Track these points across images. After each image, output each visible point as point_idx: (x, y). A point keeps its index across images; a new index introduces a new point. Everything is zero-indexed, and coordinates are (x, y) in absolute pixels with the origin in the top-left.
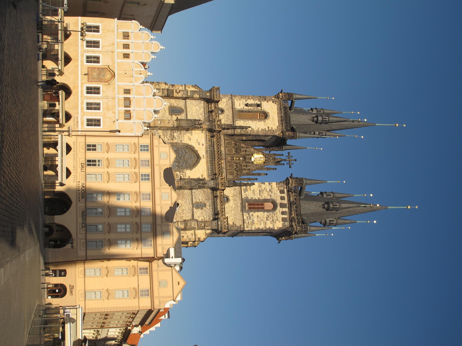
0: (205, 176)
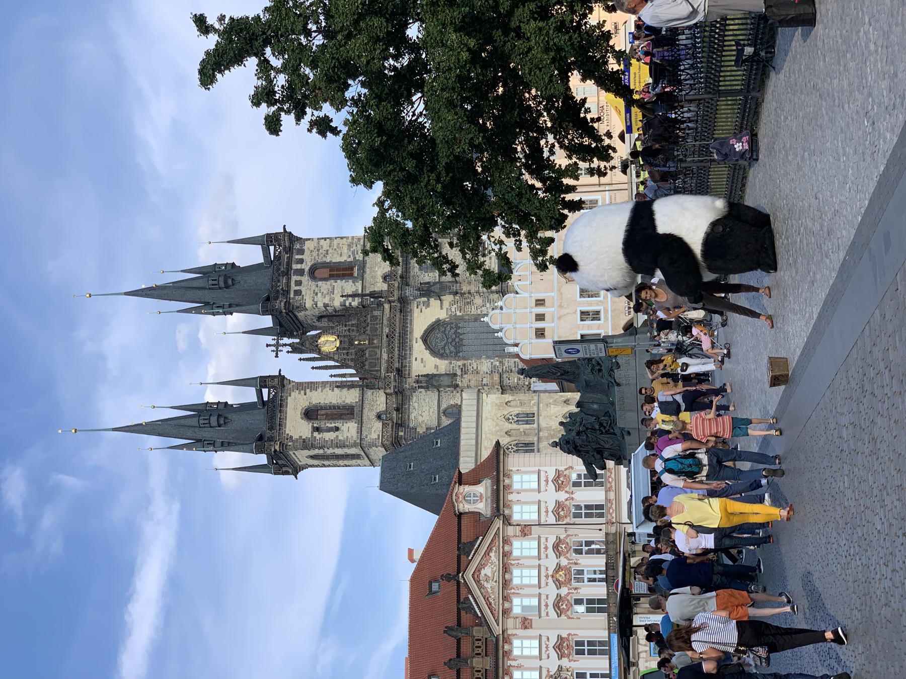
0: (416, 312)
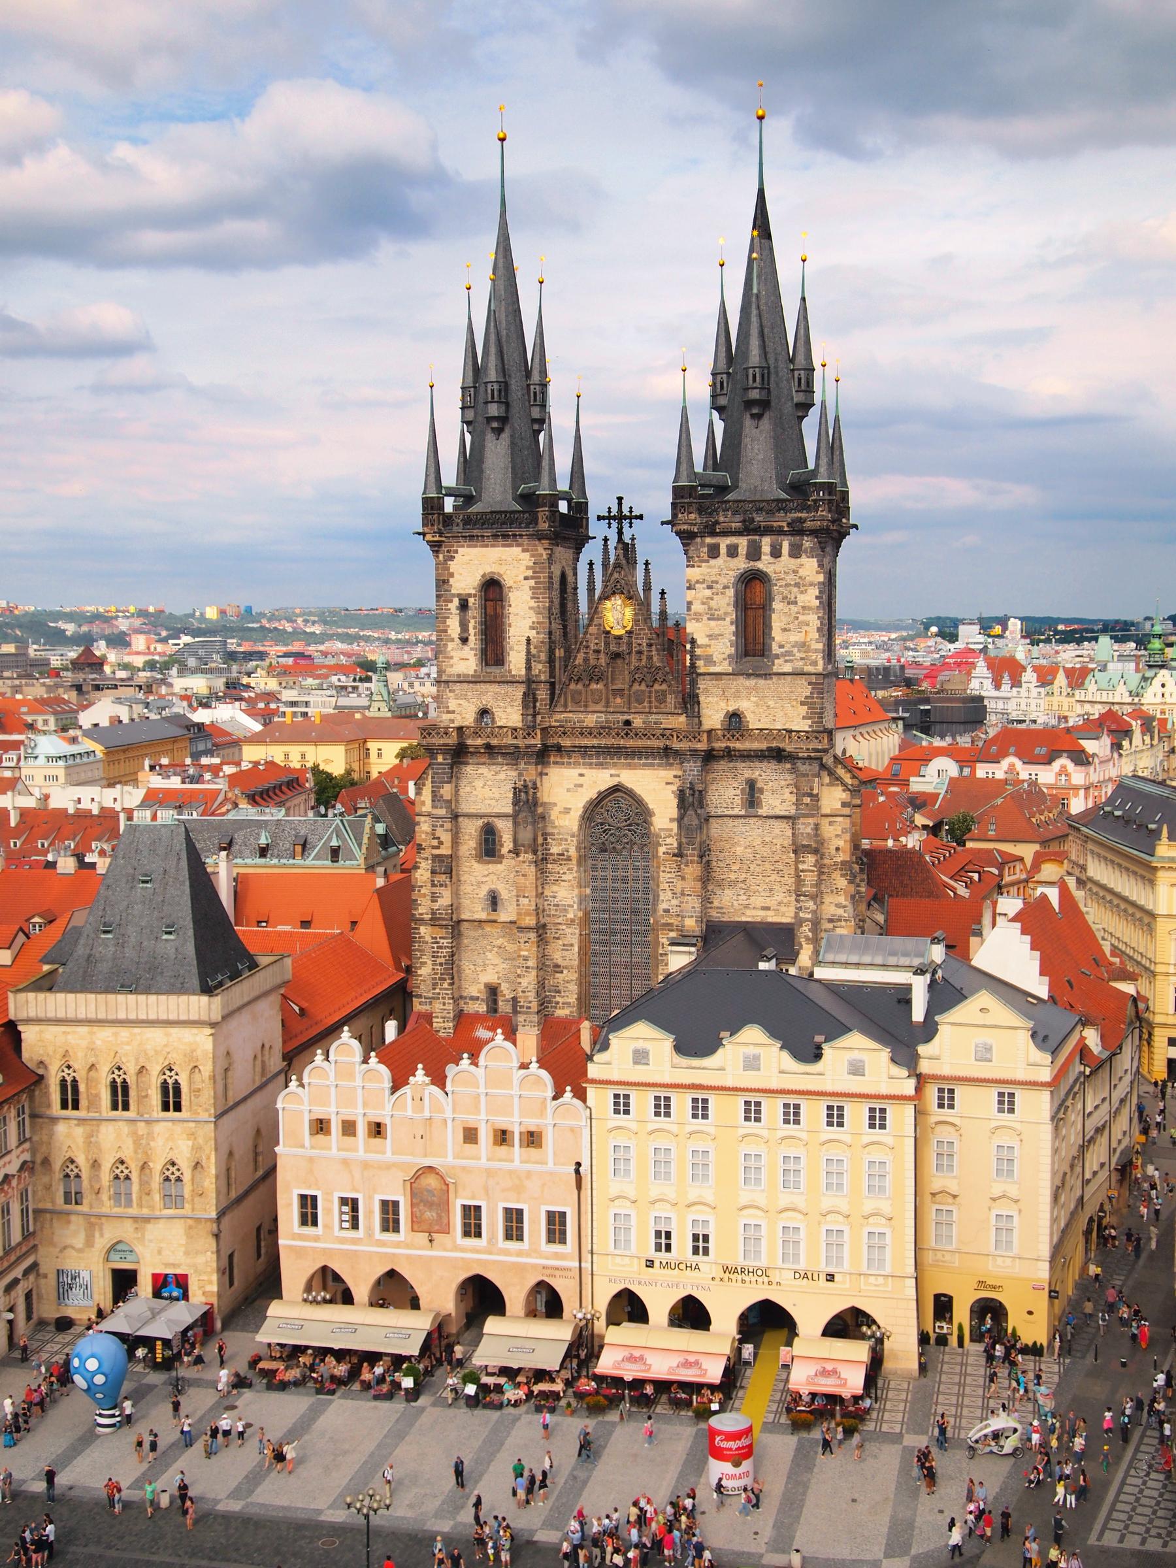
0: (668, 774)
